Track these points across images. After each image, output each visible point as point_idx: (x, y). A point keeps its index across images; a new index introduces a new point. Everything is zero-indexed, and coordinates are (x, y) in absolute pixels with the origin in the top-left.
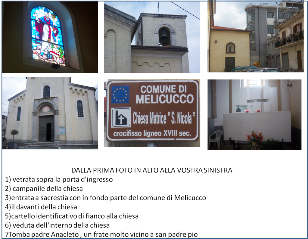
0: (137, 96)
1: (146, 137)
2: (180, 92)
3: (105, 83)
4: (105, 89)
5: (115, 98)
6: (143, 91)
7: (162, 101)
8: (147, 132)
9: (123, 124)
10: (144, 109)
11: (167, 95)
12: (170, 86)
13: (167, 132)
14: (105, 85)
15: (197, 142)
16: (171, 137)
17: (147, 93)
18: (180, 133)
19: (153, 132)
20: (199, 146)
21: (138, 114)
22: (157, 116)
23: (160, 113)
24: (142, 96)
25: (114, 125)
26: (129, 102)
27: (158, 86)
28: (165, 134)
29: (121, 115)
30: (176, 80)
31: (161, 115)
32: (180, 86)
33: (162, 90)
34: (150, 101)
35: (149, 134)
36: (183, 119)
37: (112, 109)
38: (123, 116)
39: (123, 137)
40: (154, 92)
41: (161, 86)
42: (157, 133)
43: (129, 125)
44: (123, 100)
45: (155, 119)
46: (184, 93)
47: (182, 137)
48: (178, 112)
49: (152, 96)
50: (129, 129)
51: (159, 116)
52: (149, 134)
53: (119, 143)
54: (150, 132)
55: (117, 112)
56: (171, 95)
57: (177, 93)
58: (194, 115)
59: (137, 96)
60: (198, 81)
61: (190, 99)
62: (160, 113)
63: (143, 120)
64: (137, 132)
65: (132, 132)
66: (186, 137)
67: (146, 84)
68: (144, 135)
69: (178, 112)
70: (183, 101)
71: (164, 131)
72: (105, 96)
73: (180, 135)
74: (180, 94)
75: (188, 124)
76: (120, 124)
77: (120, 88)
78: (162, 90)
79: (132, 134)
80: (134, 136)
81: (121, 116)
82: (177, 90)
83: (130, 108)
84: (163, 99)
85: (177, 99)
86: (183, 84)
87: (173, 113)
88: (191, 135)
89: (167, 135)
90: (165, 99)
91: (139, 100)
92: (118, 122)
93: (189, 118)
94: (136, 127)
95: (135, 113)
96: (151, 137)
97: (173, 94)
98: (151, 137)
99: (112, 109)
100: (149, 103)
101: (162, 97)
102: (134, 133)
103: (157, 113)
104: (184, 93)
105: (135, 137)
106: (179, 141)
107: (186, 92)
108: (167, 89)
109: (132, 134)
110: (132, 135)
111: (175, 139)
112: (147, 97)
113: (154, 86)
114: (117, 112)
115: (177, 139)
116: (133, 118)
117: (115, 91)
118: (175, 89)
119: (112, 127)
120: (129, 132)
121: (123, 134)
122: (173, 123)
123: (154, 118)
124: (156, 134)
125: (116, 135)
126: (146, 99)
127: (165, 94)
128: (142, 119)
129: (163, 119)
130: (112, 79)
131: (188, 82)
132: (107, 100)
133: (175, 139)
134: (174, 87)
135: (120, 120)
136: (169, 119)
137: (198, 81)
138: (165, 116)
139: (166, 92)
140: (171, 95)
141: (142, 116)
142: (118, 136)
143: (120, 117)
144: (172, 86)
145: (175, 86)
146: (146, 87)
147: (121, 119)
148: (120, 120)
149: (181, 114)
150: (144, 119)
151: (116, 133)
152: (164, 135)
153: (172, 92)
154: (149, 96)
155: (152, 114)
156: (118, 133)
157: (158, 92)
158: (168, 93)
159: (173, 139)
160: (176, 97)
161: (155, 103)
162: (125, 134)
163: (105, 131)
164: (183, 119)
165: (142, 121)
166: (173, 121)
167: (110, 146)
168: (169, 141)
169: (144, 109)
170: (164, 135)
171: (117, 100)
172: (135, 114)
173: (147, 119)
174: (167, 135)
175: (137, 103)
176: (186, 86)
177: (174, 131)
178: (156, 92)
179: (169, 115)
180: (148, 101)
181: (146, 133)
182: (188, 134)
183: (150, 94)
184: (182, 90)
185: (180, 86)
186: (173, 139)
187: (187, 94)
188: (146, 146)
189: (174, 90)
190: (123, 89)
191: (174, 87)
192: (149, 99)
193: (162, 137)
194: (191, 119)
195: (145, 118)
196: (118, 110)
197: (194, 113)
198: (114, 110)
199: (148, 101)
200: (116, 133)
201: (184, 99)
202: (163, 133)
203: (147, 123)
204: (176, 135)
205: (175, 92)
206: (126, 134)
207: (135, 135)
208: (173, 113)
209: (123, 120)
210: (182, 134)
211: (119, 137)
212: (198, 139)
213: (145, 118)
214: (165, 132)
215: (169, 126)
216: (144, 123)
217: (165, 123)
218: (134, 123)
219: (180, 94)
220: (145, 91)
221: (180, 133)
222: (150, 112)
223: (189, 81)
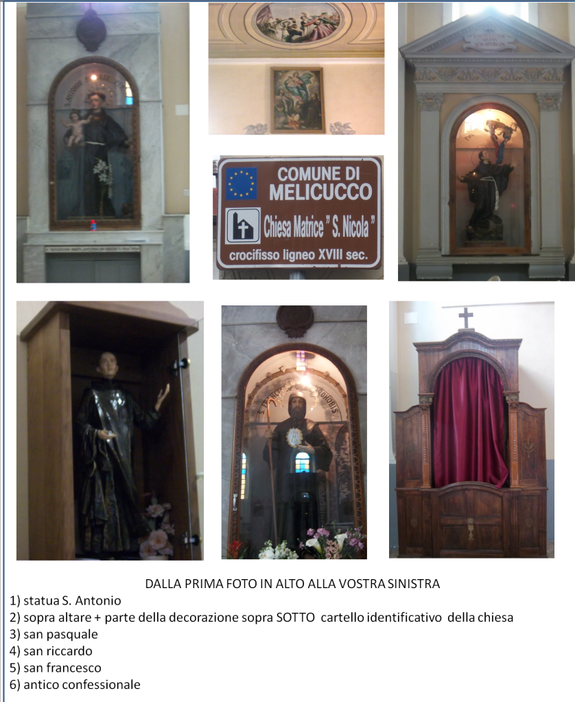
0: (272, 187)
1: (287, 262)
2: (348, 178)
3: (214, 162)
4: (214, 174)
5: (231, 190)
6: (283, 177)
7: (316, 195)
8: (289, 252)
9: (246, 238)
10: (284, 211)
11: (325, 185)
12: (329, 168)
13: (325, 252)
14: (214, 167)
15: (378, 270)
16: (332, 261)
17: (288, 182)
18: (348, 253)
19: (300, 253)
20: (382, 277)
21: (274, 220)
22: (307, 223)
23: (312, 217)
24: (281, 186)
25: (230, 239)
26: (257, 198)
27: (309, 169)
28: (322, 256)
29: (243, 221)
30: (341, 157)
31: (314, 220)
32: (348, 168)
33: (316, 176)
34: (293, 195)
35: (292, 255)
36: (353, 228)
37: (227, 209)
38: (247, 224)
39: (246, 262)
40: (301, 179)
41: (313, 168)
42: (307, 255)
43: (256, 239)
44: (247, 194)
45: (304, 228)
46: (354, 181)
47: (352, 262)
48: (344, 216)
49: (298, 186)
50: (256, 247)
51: (311, 223)
52: (292, 255)
53: (239, 272)
54: (294, 253)
55: (235, 216)
56: (332, 185)
57: (343, 180)
58: (373, 222)
59: (272, 187)
60: (379, 159)
61: (366, 192)
62: (312, 217)
63: (282, 231)
64: (271, 253)
65: (262, 252)
66: (358, 262)
67: (288, 164)
68: (284, 259)
69: (344, 216)
70: (353, 195)
71: (320, 250)
72: (215, 187)
73: (347, 258)
74: (347, 183)
75: (362, 238)
76: (240, 238)
77: (242, 172)
78: (316, 176)
79: (262, 256)
80: (265, 259)
81: (243, 223)
82: (342, 175)
83: (259, 209)
84: (317, 192)
85: (342, 191)
86: (353, 164)
87: (335, 217)
88: (367, 258)
89: (324, 258)
90: (321, 192)
91: (275, 193)
92: (237, 234)
93: (364, 227)
94: (270, 244)
95: (267, 217)
96: (297, 262)
97: (336, 183)
98: (297, 262)
99: (227, 209)
100: (293, 198)
101: (317, 189)
102: (266, 253)
103: (307, 218)
104: (354, 181)
105: (267, 262)
106: (346, 268)
107: (358, 178)
108: (326, 173)
109: (262, 256)
110: (263, 258)
111: (339, 266)
112: (290, 189)
113: (301, 169)
114: (235, 216)
115: (343, 266)
116: (264, 226)
117: (231, 178)
118: (338, 173)
119: (227, 243)
120: (257, 253)
121: (245, 256)
122: (335, 235)
123: (302, 227)
124: (305, 255)
125: (234, 258)
126: (287, 192)
127: (321, 182)
128: (280, 229)
129: (317, 229)
130: (226, 156)
131: (362, 161)
132: (217, 194)
133: (339, 266)
134: (336, 170)
135: (241, 230)
136: (328, 228)
137: (379, 159)
138: (321, 222)
139: (323, 179)
140: (332, 185)
141: (280, 222)
142: (237, 259)
143: (240, 224)
144: (334, 168)
145: (339, 168)
146: (288, 170)
147: (243, 228)
148: (241, 230)
149: (350, 220)
150: (284, 229)
151: (234, 254)
152: (320, 258)
153: (334, 179)
154: (293, 185)
155: (297, 219)
156: (238, 254)
157: (309, 179)
158: (326, 181)
159: (336, 266)
160: (341, 188)
161: (303, 198)
162: (250, 256)
163: (215, 250)
164: (353, 228)
165: (280, 232)
166: (335, 232)
167: (224, 278)
168: (328, 268)
169: (284, 211)
170: (320, 258)
171: (235, 194)
172: (267, 220)
173: (289, 229)
174: (324, 258)
175: (271, 199)
176: (358, 168)
177: (338, 250)
178: (305, 179)
179: (328, 222)
180: (290, 195)
181: (287, 255)
182: (362, 256)
183: (295, 183)
184: (350, 175)
185: (348, 168)
186: (336, 266)
187: (359, 183)
188: (288, 278)
189: (337, 176)
190: (247, 174)
191: (336, 170)
192: (292, 192)
193: (316, 261)
194: (367, 228)
195: (286, 228)
196: (238, 212)
197: (373, 217)
198: (230, 212)
199: (290, 195)
200: (234, 254)
201: (354, 192)
202: (318, 254)
203: (289, 235)
204: (341, 258)
205: (339, 179)
206: (252, 256)
207: (269, 258)
208: (335, 217)
209: (246, 230)
210: (351, 255)
211: (239, 262)
212: (381, 265)
213: (286, 228)
214: (322, 252)
215: (328, 241)
216: (284, 236)
217: (321, 235)
218: (267, 235)
219: (347, 183)
220: (286, 178)
221: (348, 253)
222: (295, 216)
223: (365, 159)
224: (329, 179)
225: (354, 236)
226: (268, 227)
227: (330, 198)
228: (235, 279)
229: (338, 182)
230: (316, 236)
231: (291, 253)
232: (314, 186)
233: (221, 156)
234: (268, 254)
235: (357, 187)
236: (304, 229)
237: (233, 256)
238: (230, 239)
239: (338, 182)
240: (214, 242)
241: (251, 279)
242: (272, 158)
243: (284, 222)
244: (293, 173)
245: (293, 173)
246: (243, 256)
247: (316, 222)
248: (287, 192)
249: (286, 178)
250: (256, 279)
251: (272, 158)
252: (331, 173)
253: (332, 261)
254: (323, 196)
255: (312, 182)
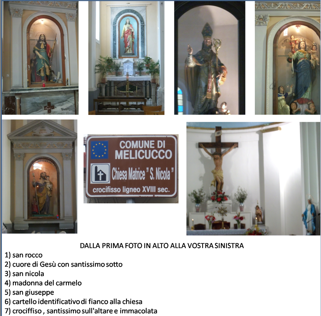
0: (117, 152)
1: (125, 193)
2: (159, 147)
3: (84, 138)
4: (84, 145)
5: (94, 153)
6: (122, 146)
7: (141, 156)
8: (126, 188)
9: (102, 180)
10: (123, 165)
11: (146, 151)
12: (148, 141)
13: (146, 188)
14: (84, 140)
15: (175, 198)
16: (150, 193)
17: (125, 149)
18: (159, 189)
19: (132, 188)
20: (177, 202)
21: (117, 170)
22: (136, 172)
23: (139, 168)
24: (121, 151)
25: (93, 181)
26: (108, 158)
27: (137, 142)
28: (144, 190)
29: (101, 171)
30: (155, 135)
31: (140, 170)
32: (159, 141)
33: (141, 146)
34: (129, 156)
35: (128, 190)
36: (161, 175)
37: (91, 164)
38: (102, 172)
39: (102, 194)
40: (132, 148)
41: (139, 141)
42: (136, 190)
43: (108, 181)
44: (103, 156)
45: (134, 174)
46: (162, 148)
47: (161, 193)
48: (156, 168)
49: (131, 151)
50: (108, 185)
51: (138, 172)
52: (128, 190)
53: (98, 199)
54: (128, 189)
55: (96, 168)
56: (150, 151)
57: (156, 148)
58: (172, 171)
59: (117, 152)
60: (176, 137)
61: (169, 154)
62: (139, 168)
63: (122, 176)
64: (116, 189)
65: (111, 188)
66: (164, 193)
67: (125, 139)
68: (123, 192)
69: (156, 168)
70: (161, 156)
71: (143, 187)
72: (85, 152)
73: (158, 191)
74: (158, 150)
75: (166, 180)
76: (99, 180)
77: (100, 143)
78: (141, 146)
79: (111, 190)
80: (113, 192)
81: (100, 172)
82: (155, 145)
83: (109, 164)
84: (142, 154)
85: (155, 154)
86: (162, 139)
87: (152, 168)
88: (169, 191)
89: (145, 191)
90: (144, 154)
91: (118, 155)
92: (97, 178)
93: (168, 174)
94: (115, 184)
95: (114, 168)
96: (130, 193)
97: (152, 150)
98: (130, 193)
99: (91, 164)
100: (128, 158)
101: (141, 153)
102: (113, 189)
103: (136, 169)
104: (162, 148)
105: (114, 193)
106: (158, 197)
107: (164, 147)
108: (146, 144)
109: (111, 190)
110: (111, 191)
111: (154, 196)
112: (126, 153)
113: (133, 142)
114: (96, 168)
115: (156, 196)
116: (112, 174)
117: (94, 147)
118: (153, 144)
119: (91, 183)
120: (108, 188)
121: (102, 190)
122: (151, 179)
123: (133, 174)
124: (135, 190)
125: (95, 191)
126: (125, 154)
127: (143, 149)
128: (121, 175)
129: (141, 175)
130: (91, 135)
131: (167, 138)
132: (86, 156)
133: (154, 196)
134: (152, 143)
135: (99, 176)
136: (148, 175)
137: (176, 137)
138: (144, 172)
139: (145, 147)
140: (150, 151)
141: (121, 172)
142: (97, 192)
143: (99, 172)
144: (151, 141)
145: (154, 141)
146: (125, 142)
147: (100, 174)
148: (99, 176)
149: (160, 170)
150: (123, 175)
151: (95, 189)
152: (143, 191)
153: (151, 147)
154: (128, 151)
155: (130, 170)
156: (97, 189)
157: (137, 147)
158: (147, 149)
159: (152, 196)
160: (155, 152)
161: (134, 158)
162: (104, 190)
163: (85, 187)
164: (161, 175)
165: (121, 177)
166: (152, 177)
167: (90, 203)
168: (148, 197)
169: (123, 165)
170: (143, 191)
171: (96, 156)
172: (114, 170)
173: (126, 175)
174: (145, 191)
175: (116, 158)
176: (164, 141)
177: (153, 187)
178: (135, 148)
179: (147, 171)
180: (127, 156)
181: (125, 189)
182: (166, 190)
183: (129, 149)
184: (160, 145)
185: (159, 141)
186: (152, 196)
187: (165, 150)
188: (125, 202)
189: (152, 146)
190: (103, 144)
191: (152, 143)
192: (128, 154)
193: (141, 193)
194: (169, 175)
195: (124, 174)
196: (97, 166)
197: (172, 169)
198: (93, 166)
199: (127, 156)
200: (95, 189)
201: (162, 154)
202: (142, 189)
203: (126, 179)
204: (155, 191)
205: (154, 147)
206: (105, 190)
207: (115, 192)
208: (152, 168)
209: (102, 176)
210: (160, 190)
211: (98, 194)
212: (177, 195)
213: (124, 174)
214: (144, 188)
215: (147, 182)
216: (123, 179)
217: (144, 179)
218: (114, 179)
219: (158, 150)
220: (124, 147)
221: (159, 189)
222: (129, 168)
223: (168, 136)
224: (148, 147)
225: (162, 179)
226: (114, 174)
227: (149, 158)
228: (96, 203)
229: (153, 149)
230: (141, 179)
231: (127, 188)
232: (142, 147)
233: (88, 135)
234: (114, 189)
235: (164, 152)
236: (134, 175)
237: (95, 190)
238: (93, 181)
239: (153, 149)
240: (84, 182)
241: (105, 203)
242: (117, 136)
243: (123, 171)
244: (128, 144)
245: (128, 144)
246: (100, 190)
247: (141, 171)
248: (125, 154)
249: (124, 147)
250: (107, 203)
251: (117, 136)
252: (149, 144)
253: (150, 193)
254: (145, 157)
255: (138, 149)
